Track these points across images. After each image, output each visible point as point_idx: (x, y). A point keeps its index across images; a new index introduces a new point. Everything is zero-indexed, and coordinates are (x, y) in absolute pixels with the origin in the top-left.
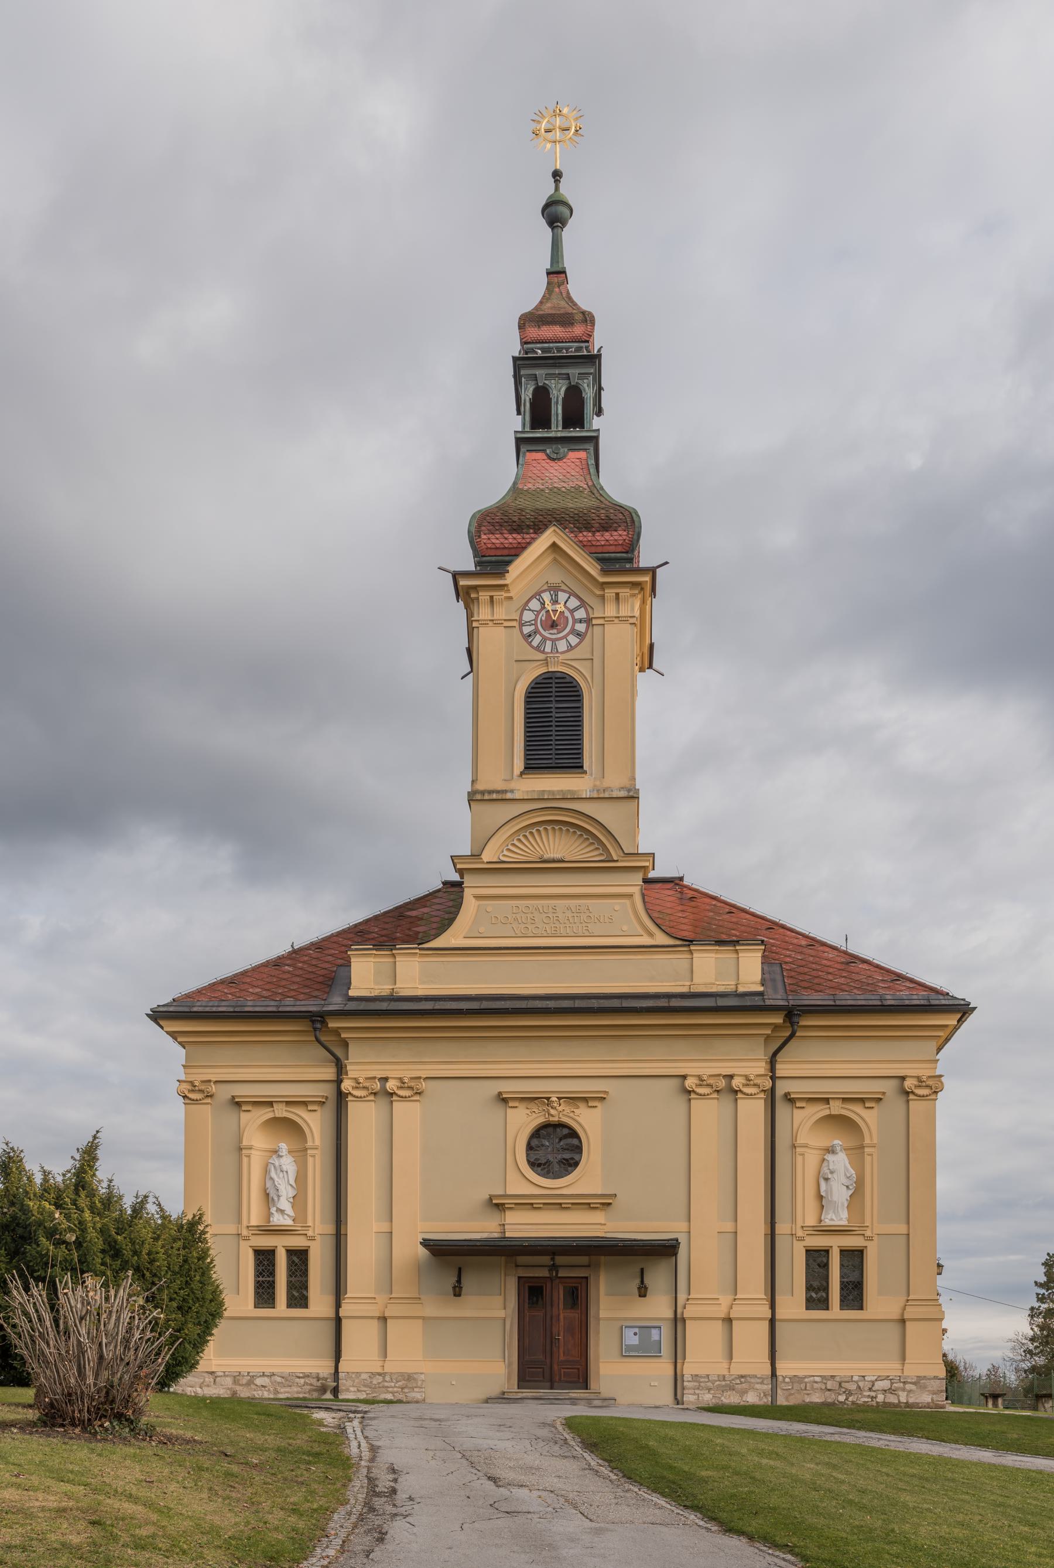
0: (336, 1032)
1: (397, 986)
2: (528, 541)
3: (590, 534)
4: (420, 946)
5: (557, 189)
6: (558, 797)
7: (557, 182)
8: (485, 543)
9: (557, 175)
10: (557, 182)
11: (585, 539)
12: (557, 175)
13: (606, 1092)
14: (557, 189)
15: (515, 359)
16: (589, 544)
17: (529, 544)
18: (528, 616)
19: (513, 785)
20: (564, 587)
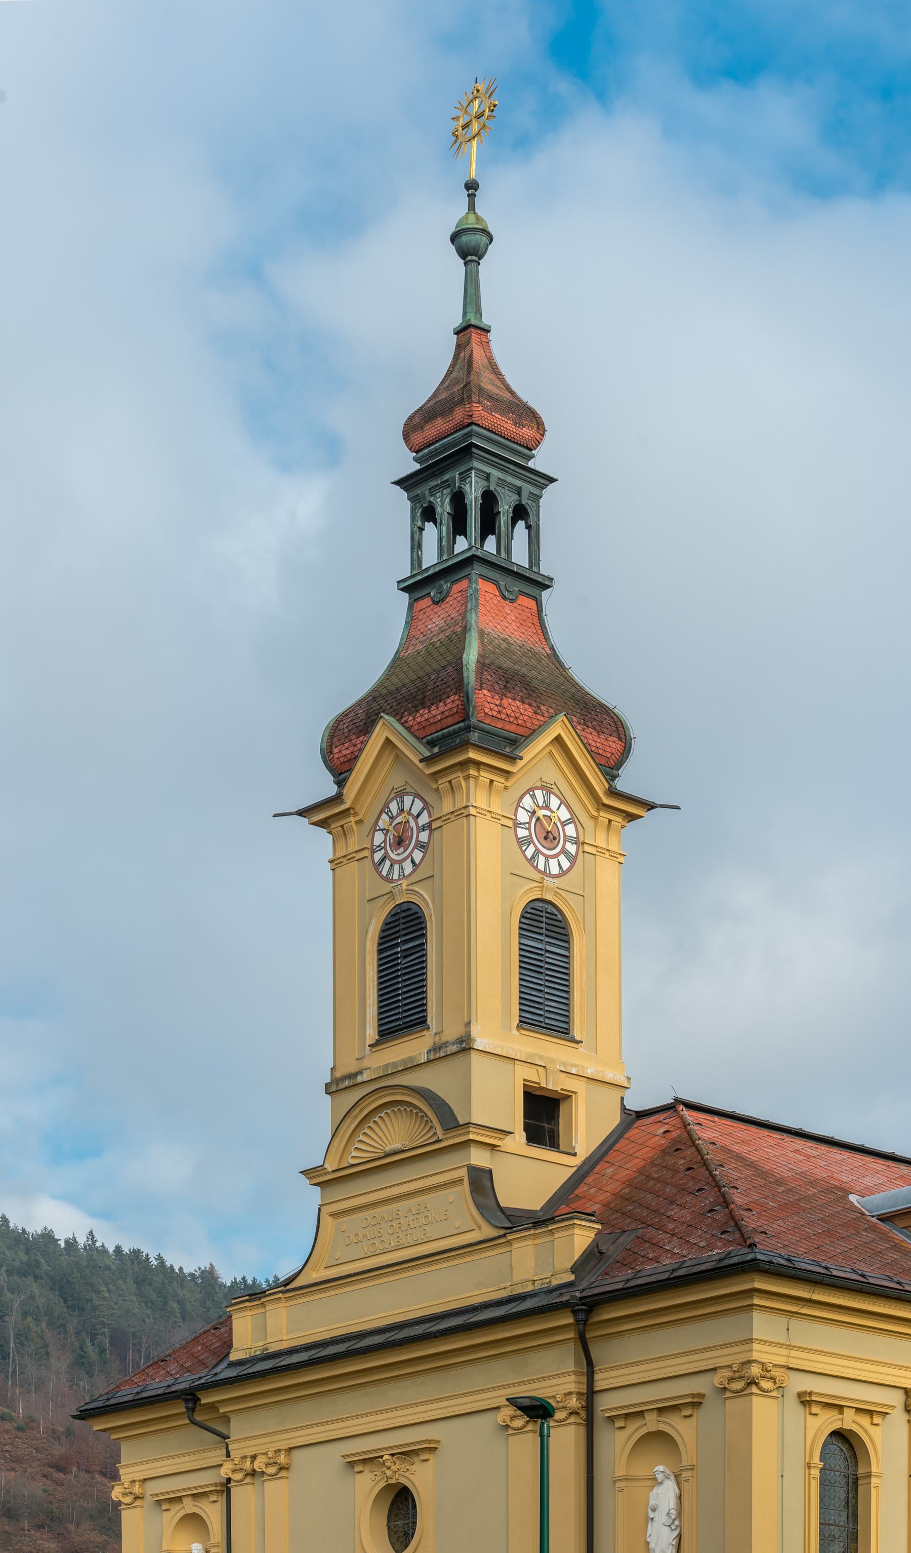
0: (213, 1407)
1: (269, 1340)
2: (359, 746)
3: (426, 711)
4: (288, 1288)
5: (472, 207)
6: (400, 1069)
7: (472, 197)
8: (337, 758)
9: (472, 187)
10: (472, 197)
11: (423, 719)
12: (472, 187)
13: (438, 1442)
14: (472, 207)
15: (405, 483)
16: (428, 723)
17: (361, 750)
18: (379, 838)
19: (366, 1063)
20: (409, 789)
